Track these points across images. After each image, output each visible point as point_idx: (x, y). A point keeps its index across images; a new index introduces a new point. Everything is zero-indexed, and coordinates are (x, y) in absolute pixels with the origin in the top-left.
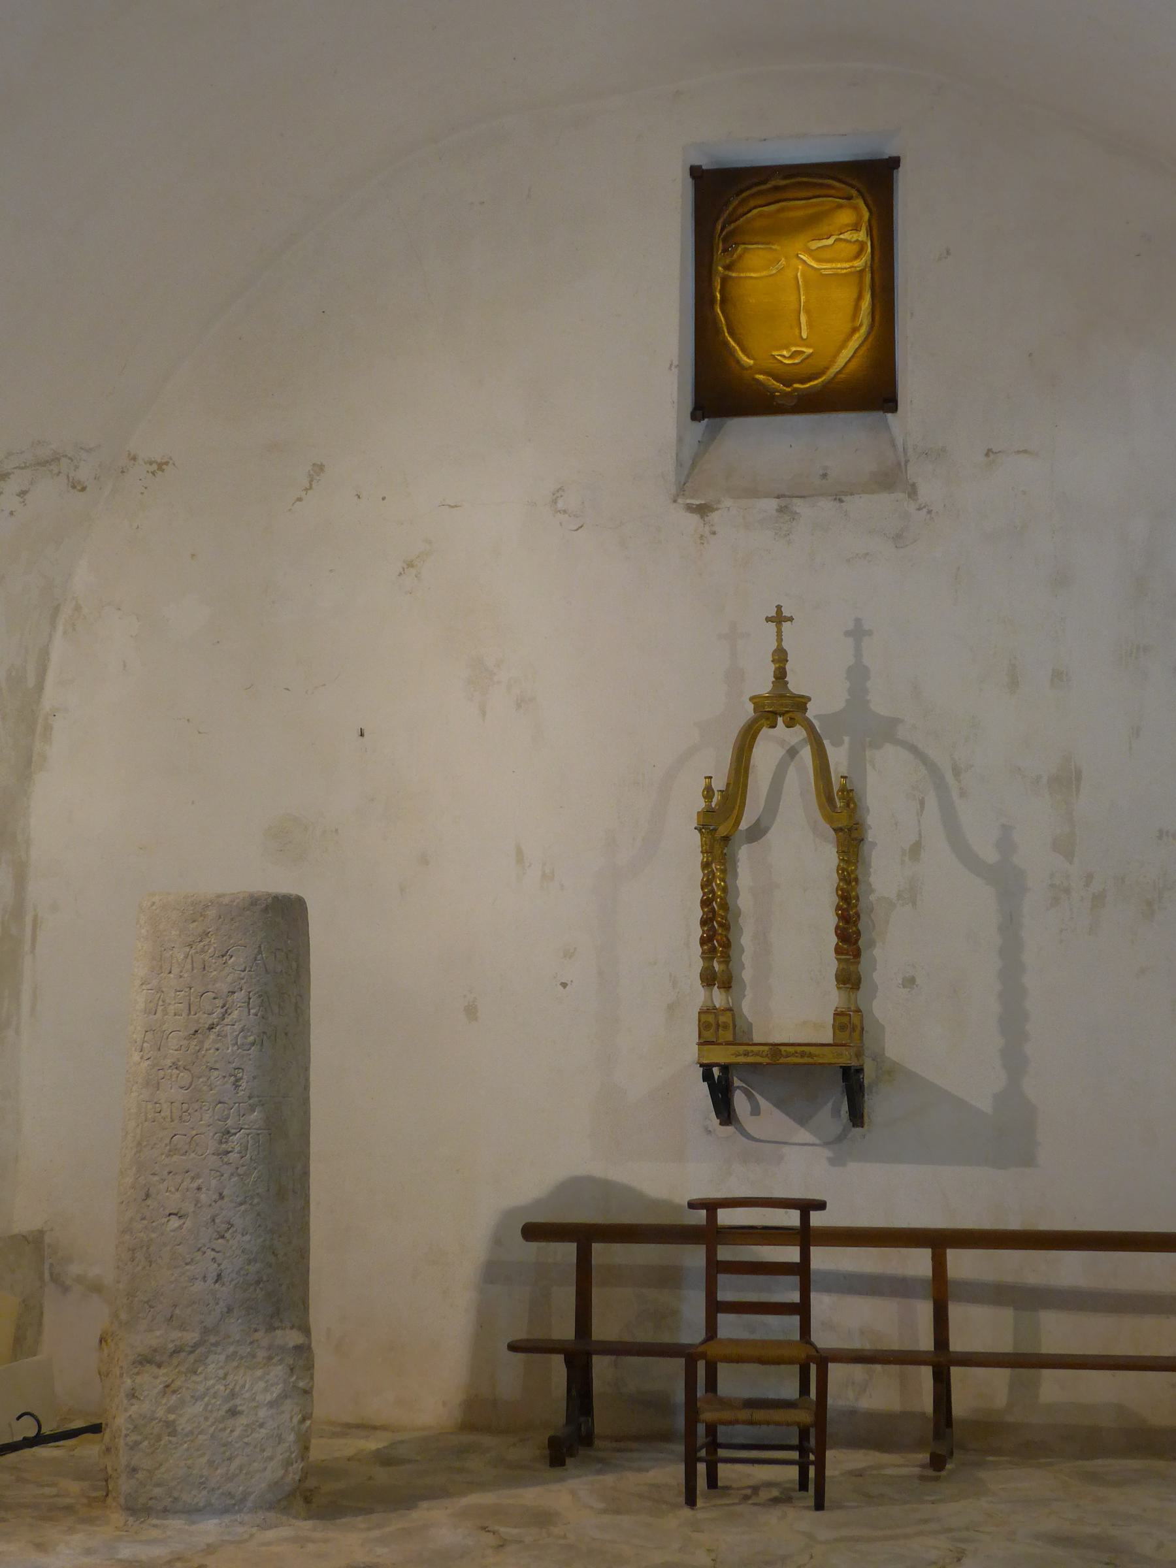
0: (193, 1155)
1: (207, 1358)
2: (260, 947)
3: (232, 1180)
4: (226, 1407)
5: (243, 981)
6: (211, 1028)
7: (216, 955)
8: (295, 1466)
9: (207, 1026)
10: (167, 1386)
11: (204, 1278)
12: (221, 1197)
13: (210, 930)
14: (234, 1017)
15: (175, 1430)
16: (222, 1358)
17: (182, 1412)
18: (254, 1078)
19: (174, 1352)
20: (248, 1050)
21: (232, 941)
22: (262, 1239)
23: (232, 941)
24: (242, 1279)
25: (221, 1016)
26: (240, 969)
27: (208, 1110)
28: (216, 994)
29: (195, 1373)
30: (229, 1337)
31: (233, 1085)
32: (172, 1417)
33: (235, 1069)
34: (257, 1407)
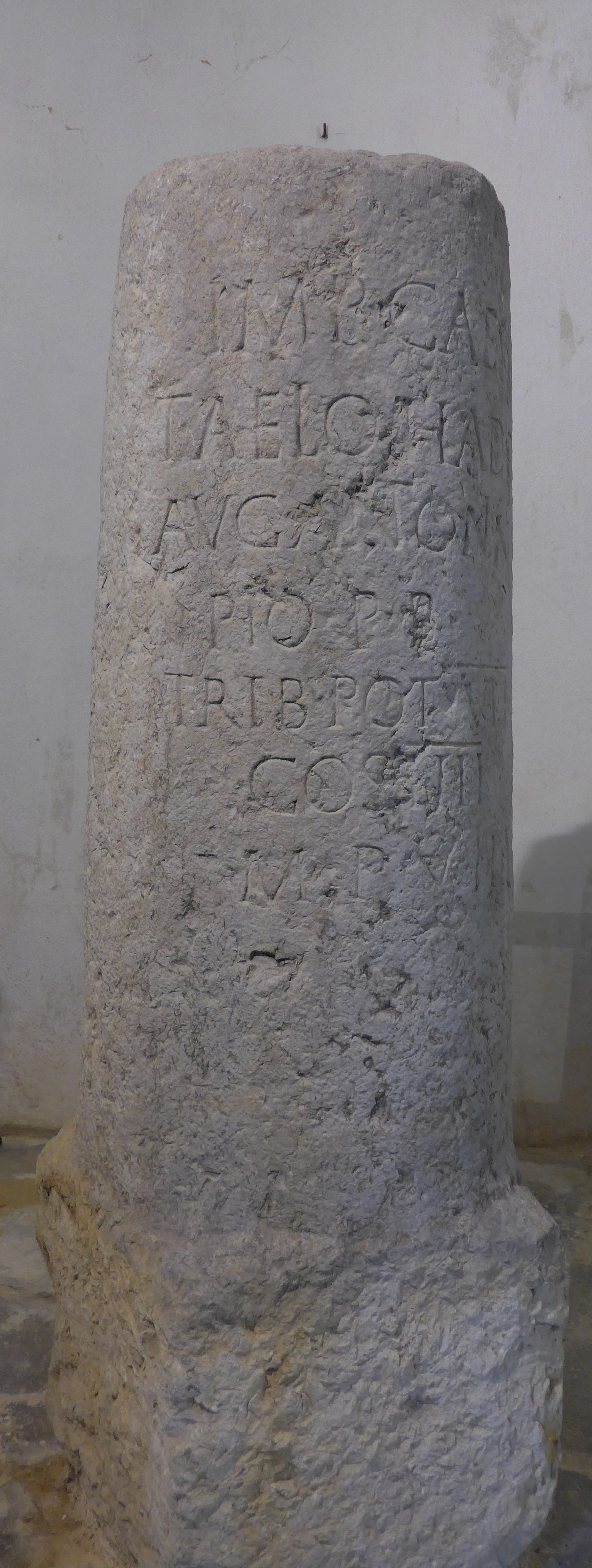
0: (312, 809)
1: (359, 1292)
2: (461, 294)
3: (408, 869)
4: (399, 1397)
5: (429, 375)
6: (354, 489)
7: (364, 301)
8: (540, 1493)
9: (345, 483)
10: (271, 1371)
11: (347, 1108)
12: (384, 909)
13: (347, 235)
14: (410, 462)
15: (291, 1465)
16: (392, 1287)
17: (305, 1424)
18: (453, 618)
19: (286, 1289)
20: (439, 550)
21: (402, 270)
22: (466, 1003)
23: (402, 270)
24: (429, 1100)
25: (379, 457)
26: (422, 343)
27: (351, 697)
28: (368, 402)
29: (333, 1330)
30: (406, 1236)
31: (410, 633)
32: (283, 1439)
33: (413, 594)
34: (465, 1384)
